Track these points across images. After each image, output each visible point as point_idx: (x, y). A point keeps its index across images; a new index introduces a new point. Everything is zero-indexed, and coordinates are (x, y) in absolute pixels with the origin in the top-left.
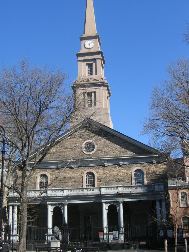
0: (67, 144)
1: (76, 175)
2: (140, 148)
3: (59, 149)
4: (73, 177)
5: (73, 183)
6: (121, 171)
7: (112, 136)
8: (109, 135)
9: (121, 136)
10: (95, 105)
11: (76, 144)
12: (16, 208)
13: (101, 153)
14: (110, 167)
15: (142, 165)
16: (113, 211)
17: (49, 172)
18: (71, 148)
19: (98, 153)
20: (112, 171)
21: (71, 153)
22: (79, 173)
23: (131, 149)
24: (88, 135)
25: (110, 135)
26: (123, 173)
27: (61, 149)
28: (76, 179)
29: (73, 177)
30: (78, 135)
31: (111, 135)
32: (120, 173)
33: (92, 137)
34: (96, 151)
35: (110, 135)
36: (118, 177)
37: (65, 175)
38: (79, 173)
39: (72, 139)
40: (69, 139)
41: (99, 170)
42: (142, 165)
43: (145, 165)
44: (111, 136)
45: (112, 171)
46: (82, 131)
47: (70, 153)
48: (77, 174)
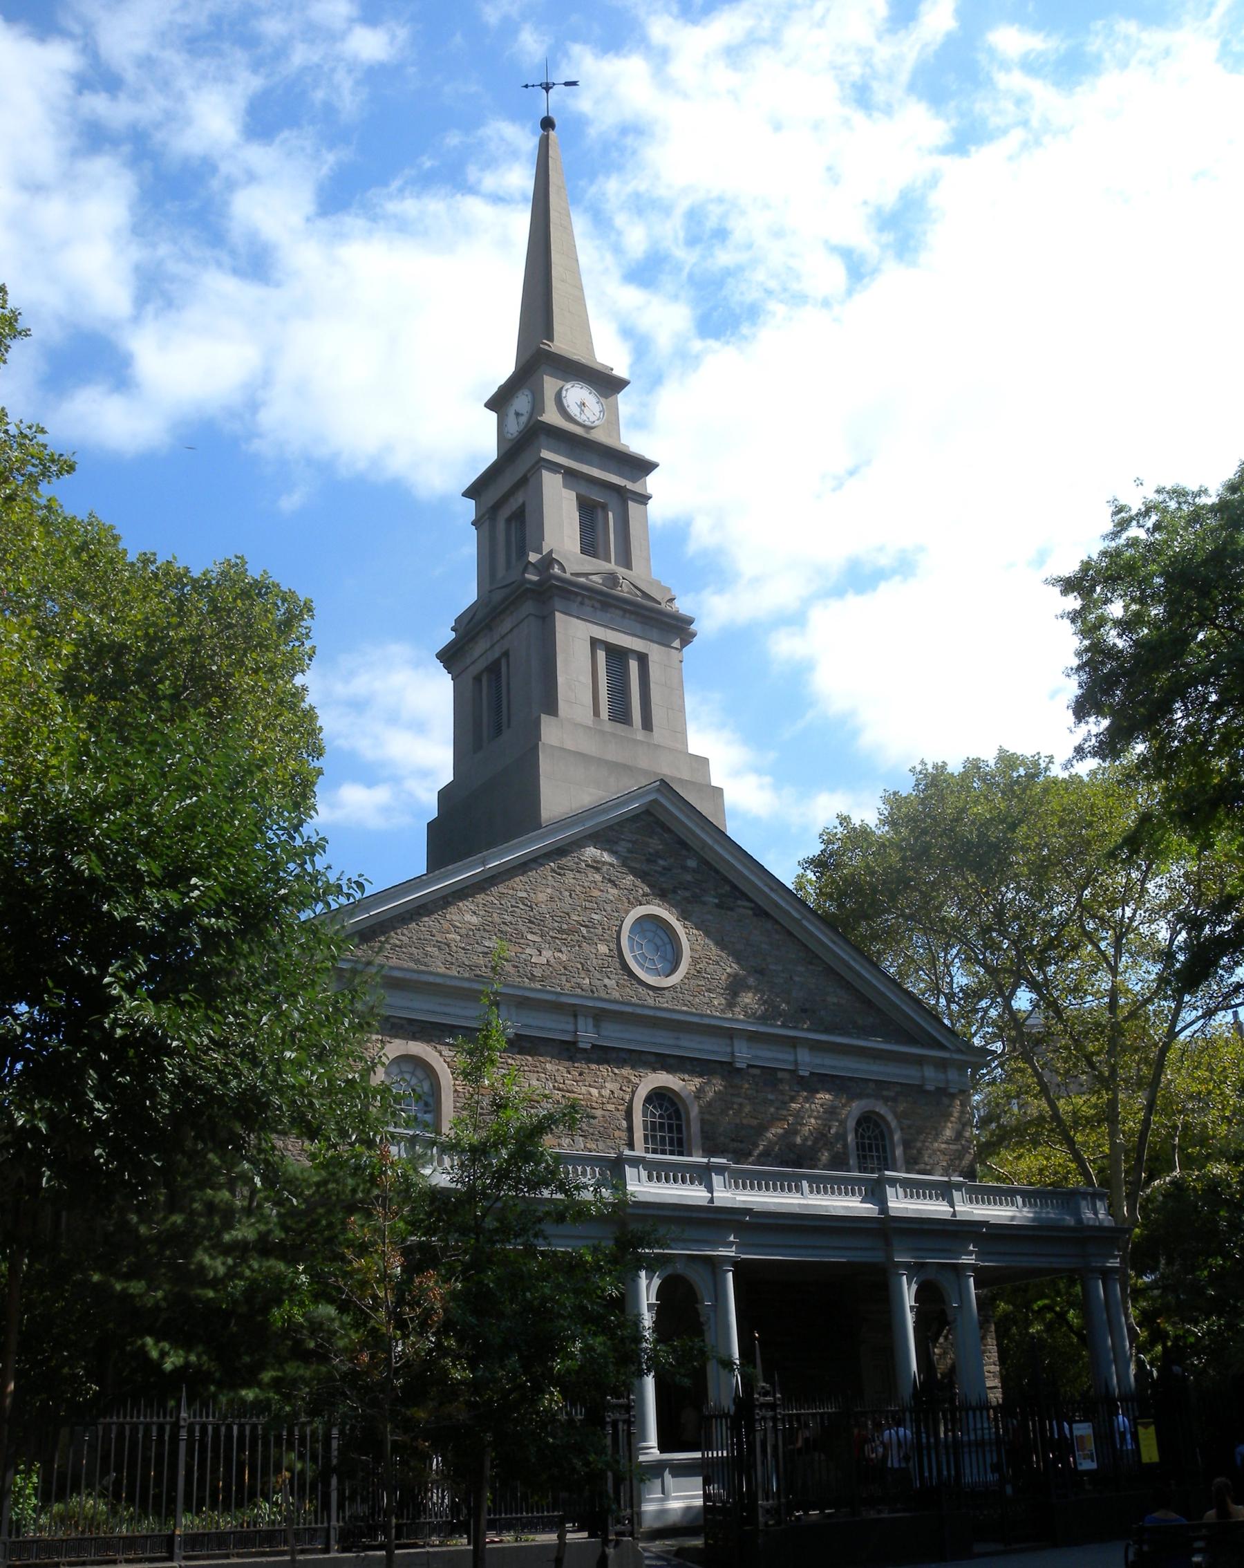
0: (542, 897)
1: (595, 1092)
2: (868, 1003)
3: (497, 919)
8: (739, 902)
9: (805, 923)
10: (647, 725)
13: (709, 991)
15: (885, 1093)
17: (446, 1052)
18: (565, 927)
21: (564, 958)
23: (835, 1000)
27: (508, 918)
30: (597, 862)
34: (687, 977)
35: (744, 907)
40: (553, 871)
42: (885, 1093)
47: (560, 954)
48: (602, 1087)
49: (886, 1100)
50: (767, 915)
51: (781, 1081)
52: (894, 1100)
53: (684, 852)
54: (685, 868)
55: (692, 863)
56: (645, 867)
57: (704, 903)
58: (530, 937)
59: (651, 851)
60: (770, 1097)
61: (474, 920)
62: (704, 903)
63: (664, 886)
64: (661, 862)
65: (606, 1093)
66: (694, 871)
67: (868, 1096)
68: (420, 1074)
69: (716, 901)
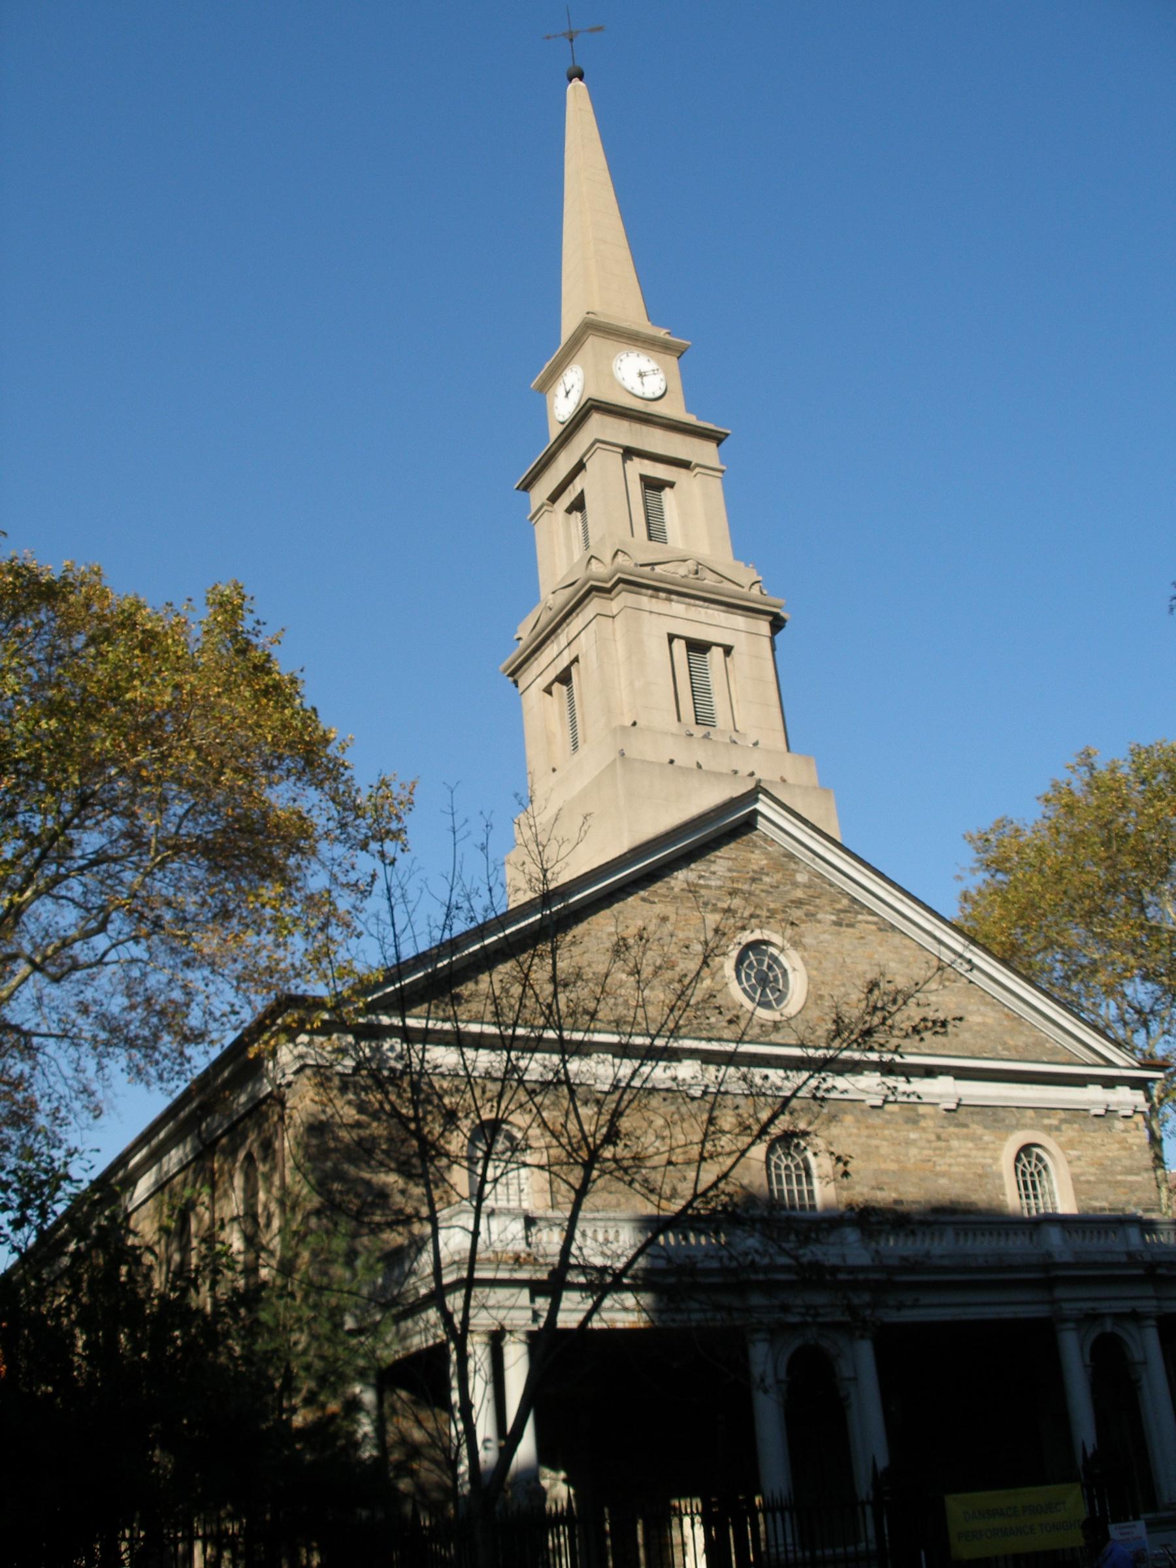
6: (949, 1149)
7: (880, 930)
8: (860, 917)
14: (892, 1113)
15: (1046, 1121)
20: (909, 1143)
25: (871, 918)
26: (963, 1160)
31: (875, 919)
32: (948, 1160)
35: (867, 922)
42: (1046, 1121)
43: (1054, 1122)
44: (874, 927)
45: (909, 1143)
46: (714, 862)
49: (1048, 1129)
50: (893, 927)
51: (924, 1116)
52: (1058, 1129)
53: (793, 866)
54: (795, 885)
55: (801, 878)
57: (819, 922)
59: (755, 868)
60: (913, 1136)
62: (819, 922)
63: (772, 906)
64: (766, 879)
66: (805, 886)
67: (1025, 1126)
69: (834, 918)
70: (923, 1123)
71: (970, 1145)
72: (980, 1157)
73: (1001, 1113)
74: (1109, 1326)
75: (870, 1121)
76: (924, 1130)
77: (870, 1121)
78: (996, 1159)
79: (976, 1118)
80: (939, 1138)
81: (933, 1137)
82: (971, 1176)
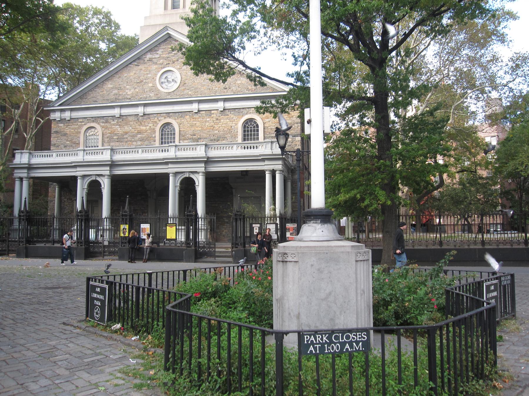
0: (132, 74)
1: (144, 128)
4: (139, 132)
5: (139, 143)
11: (147, 74)
12: (25, 183)
16: (188, 186)
17: (102, 124)
19: (184, 90)
20: (206, 122)
21: (137, 90)
22: (150, 125)
23: (240, 82)
24: (168, 57)
28: (144, 136)
29: (139, 132)
32: (219, 126)
33: (174, 63)
36: (216, 132)
37: (127, 128)
38: (150, 125)
39: (140, 67)
41: (183, 120)
51: (213, 114)
56: (167, 56)
58: (128, 87)
61: (111, 86)
65: (148, 127)
68: (93, 130)
70: (212, 116)
71: (228, 120)
72: (230, 124)
73: (242, 110)
74: (187, 175)
75: (195, 117)
76: (213, 117)
77: (195, 117)
78: (236, 124)
79: (232, 113)
80: (217, 119)
81: (215, 119)
82: (226, 129)
